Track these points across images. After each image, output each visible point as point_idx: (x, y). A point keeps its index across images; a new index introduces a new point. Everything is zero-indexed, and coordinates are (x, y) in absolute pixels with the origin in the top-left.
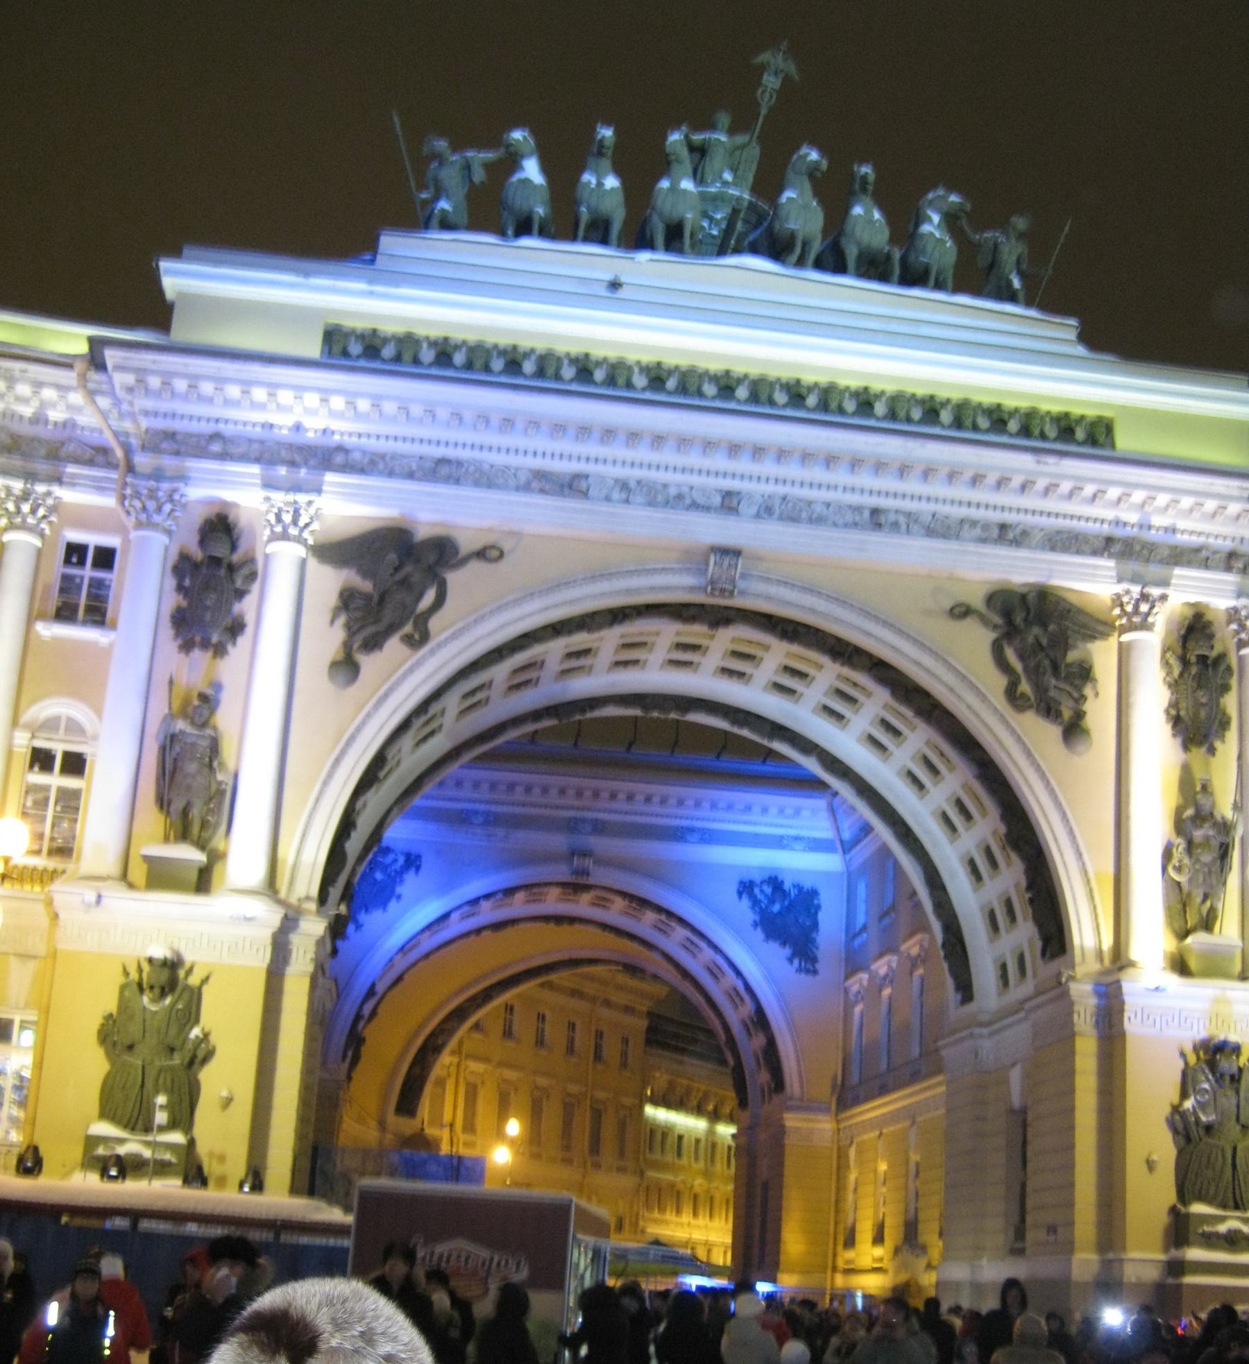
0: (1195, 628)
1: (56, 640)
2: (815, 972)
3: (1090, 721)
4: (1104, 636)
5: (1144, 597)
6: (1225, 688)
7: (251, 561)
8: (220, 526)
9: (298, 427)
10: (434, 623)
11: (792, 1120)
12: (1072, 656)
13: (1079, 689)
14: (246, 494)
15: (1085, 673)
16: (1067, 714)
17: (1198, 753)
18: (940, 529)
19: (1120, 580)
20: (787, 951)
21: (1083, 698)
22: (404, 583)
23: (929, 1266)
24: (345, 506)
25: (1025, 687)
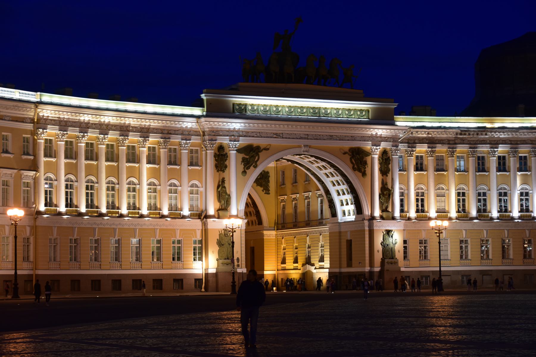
0: (384, 153)
1: (192, 169)
2: (269, 194)
3: (367, 172)
4: (369, 155)
5: (377, 149)
6: (389, 163)
8: (221, 148)
9: (235, 128)
10: (258, 163)
11: (265, 232)
13: (365, 166)
14: (225, 141)
15: (366, 163)
16: (363, 171)
18: (341, 139)
19: (372, 146)
20: (262, 189)
22: (252, 156)
23: (315, 268)
24: (243, 142)
25: (356, 166)
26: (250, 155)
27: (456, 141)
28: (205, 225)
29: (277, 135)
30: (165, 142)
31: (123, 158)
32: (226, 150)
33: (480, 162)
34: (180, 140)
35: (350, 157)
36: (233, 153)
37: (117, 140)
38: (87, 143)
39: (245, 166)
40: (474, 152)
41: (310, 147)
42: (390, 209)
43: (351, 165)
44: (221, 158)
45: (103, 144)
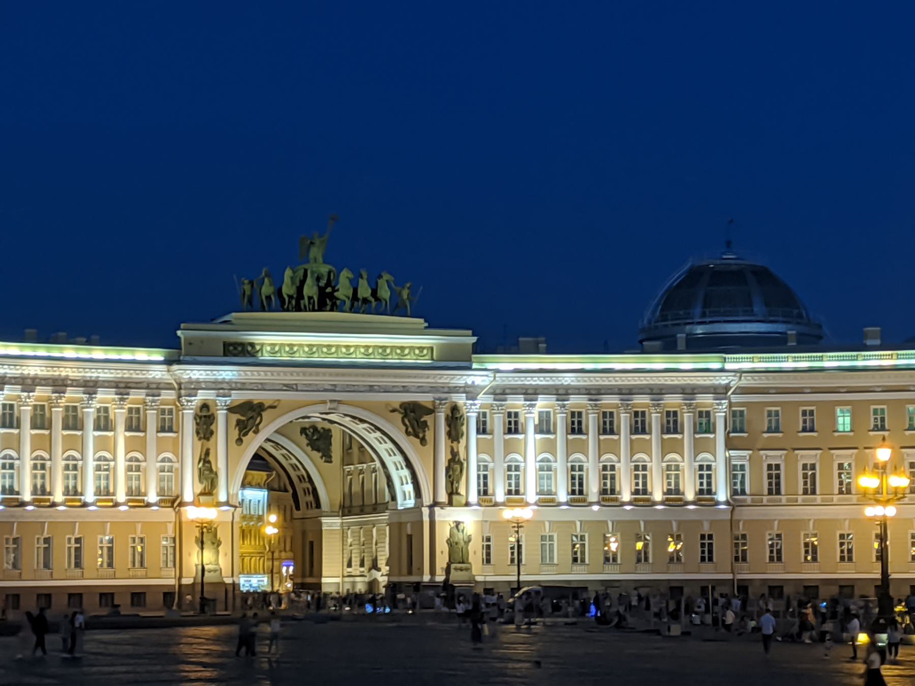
3: (427, 438)
7: (213, 414)
10: (261, 426)
12: (422, 420)
17: (455, 443)
21: (424, 431)
22: (252, 417)
25: (410, 429)
26: (248, 416)
27: (570, 391)
28: (179, 514)
29: (289, 387)
30: (121, 400)
31: (58, 423)
32: (212, 410)
33: (608, 420)
34: (143, 397)
35: (401, 416)
36: (221, 415)
37: (49, 399)
38: (35, 407)
39: (240, 431)
40: (596, 405)
41: (339, 402)
42: (462, 491)
43: (404, 428)
44: (205, 421)
45: (59, 407)
